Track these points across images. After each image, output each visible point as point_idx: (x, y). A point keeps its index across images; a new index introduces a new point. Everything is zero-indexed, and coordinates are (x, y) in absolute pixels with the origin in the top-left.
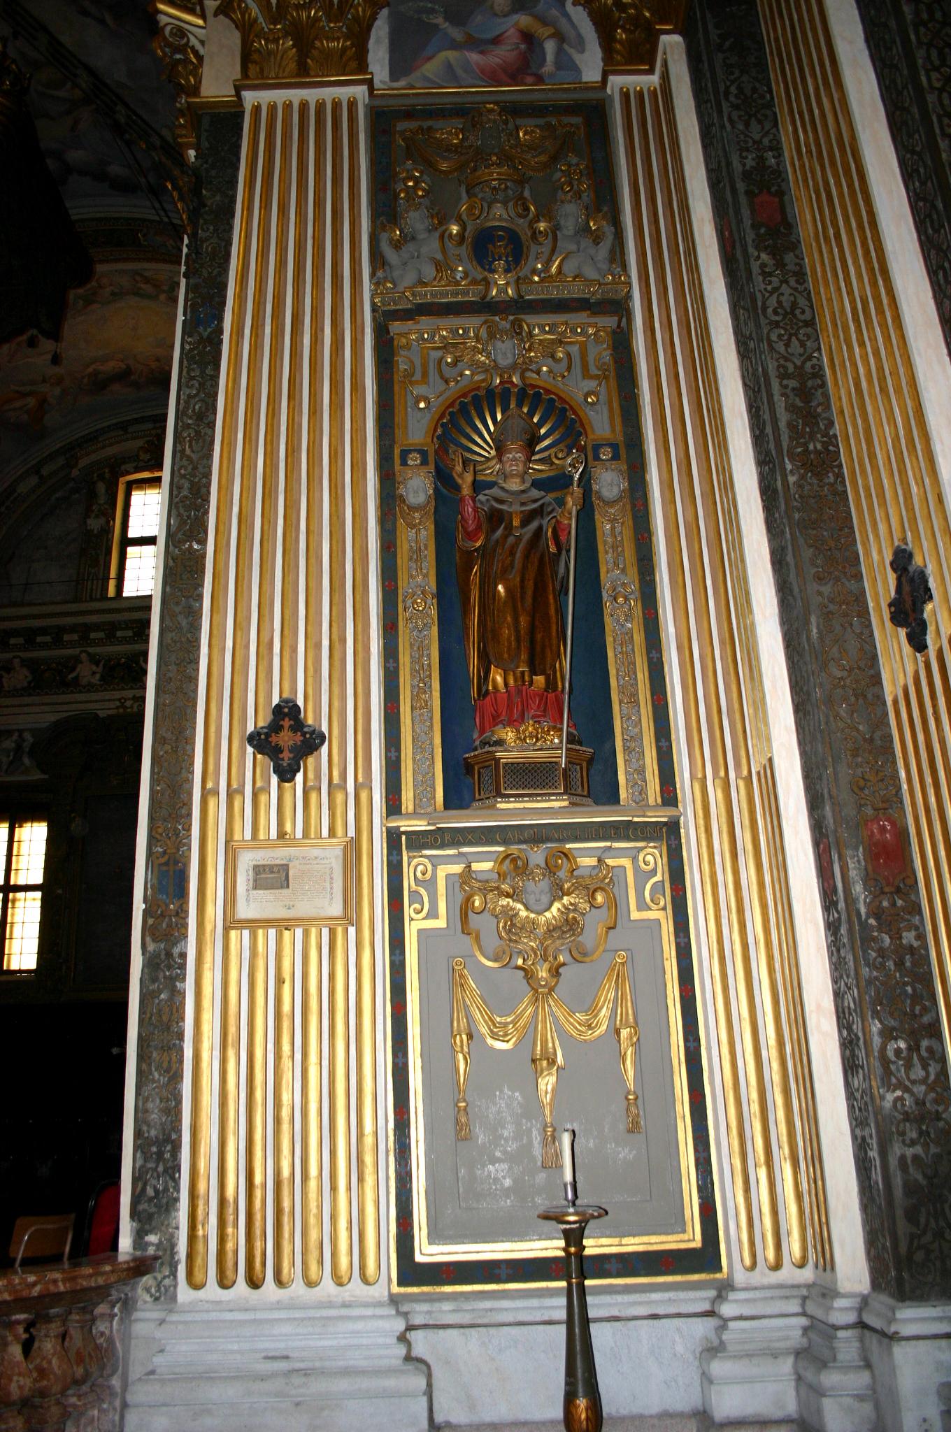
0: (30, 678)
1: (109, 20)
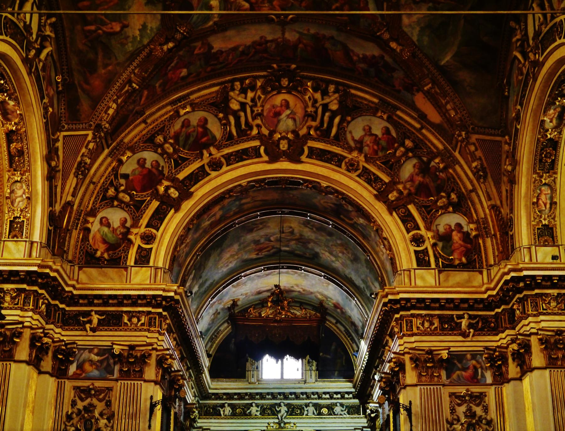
0: (231, 412)
1: (314, 229)
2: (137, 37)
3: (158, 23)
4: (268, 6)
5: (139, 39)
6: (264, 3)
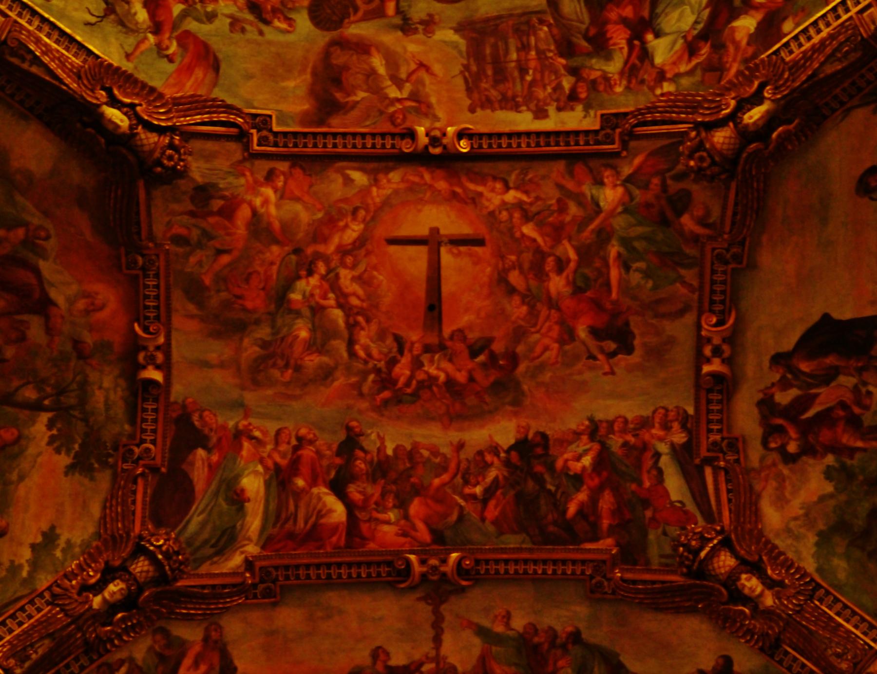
2: (21, 566)
3: (91, 529)
4: (396, 523)
5: (24, 574)
6: (386, 510)
